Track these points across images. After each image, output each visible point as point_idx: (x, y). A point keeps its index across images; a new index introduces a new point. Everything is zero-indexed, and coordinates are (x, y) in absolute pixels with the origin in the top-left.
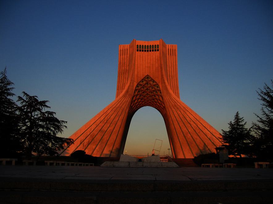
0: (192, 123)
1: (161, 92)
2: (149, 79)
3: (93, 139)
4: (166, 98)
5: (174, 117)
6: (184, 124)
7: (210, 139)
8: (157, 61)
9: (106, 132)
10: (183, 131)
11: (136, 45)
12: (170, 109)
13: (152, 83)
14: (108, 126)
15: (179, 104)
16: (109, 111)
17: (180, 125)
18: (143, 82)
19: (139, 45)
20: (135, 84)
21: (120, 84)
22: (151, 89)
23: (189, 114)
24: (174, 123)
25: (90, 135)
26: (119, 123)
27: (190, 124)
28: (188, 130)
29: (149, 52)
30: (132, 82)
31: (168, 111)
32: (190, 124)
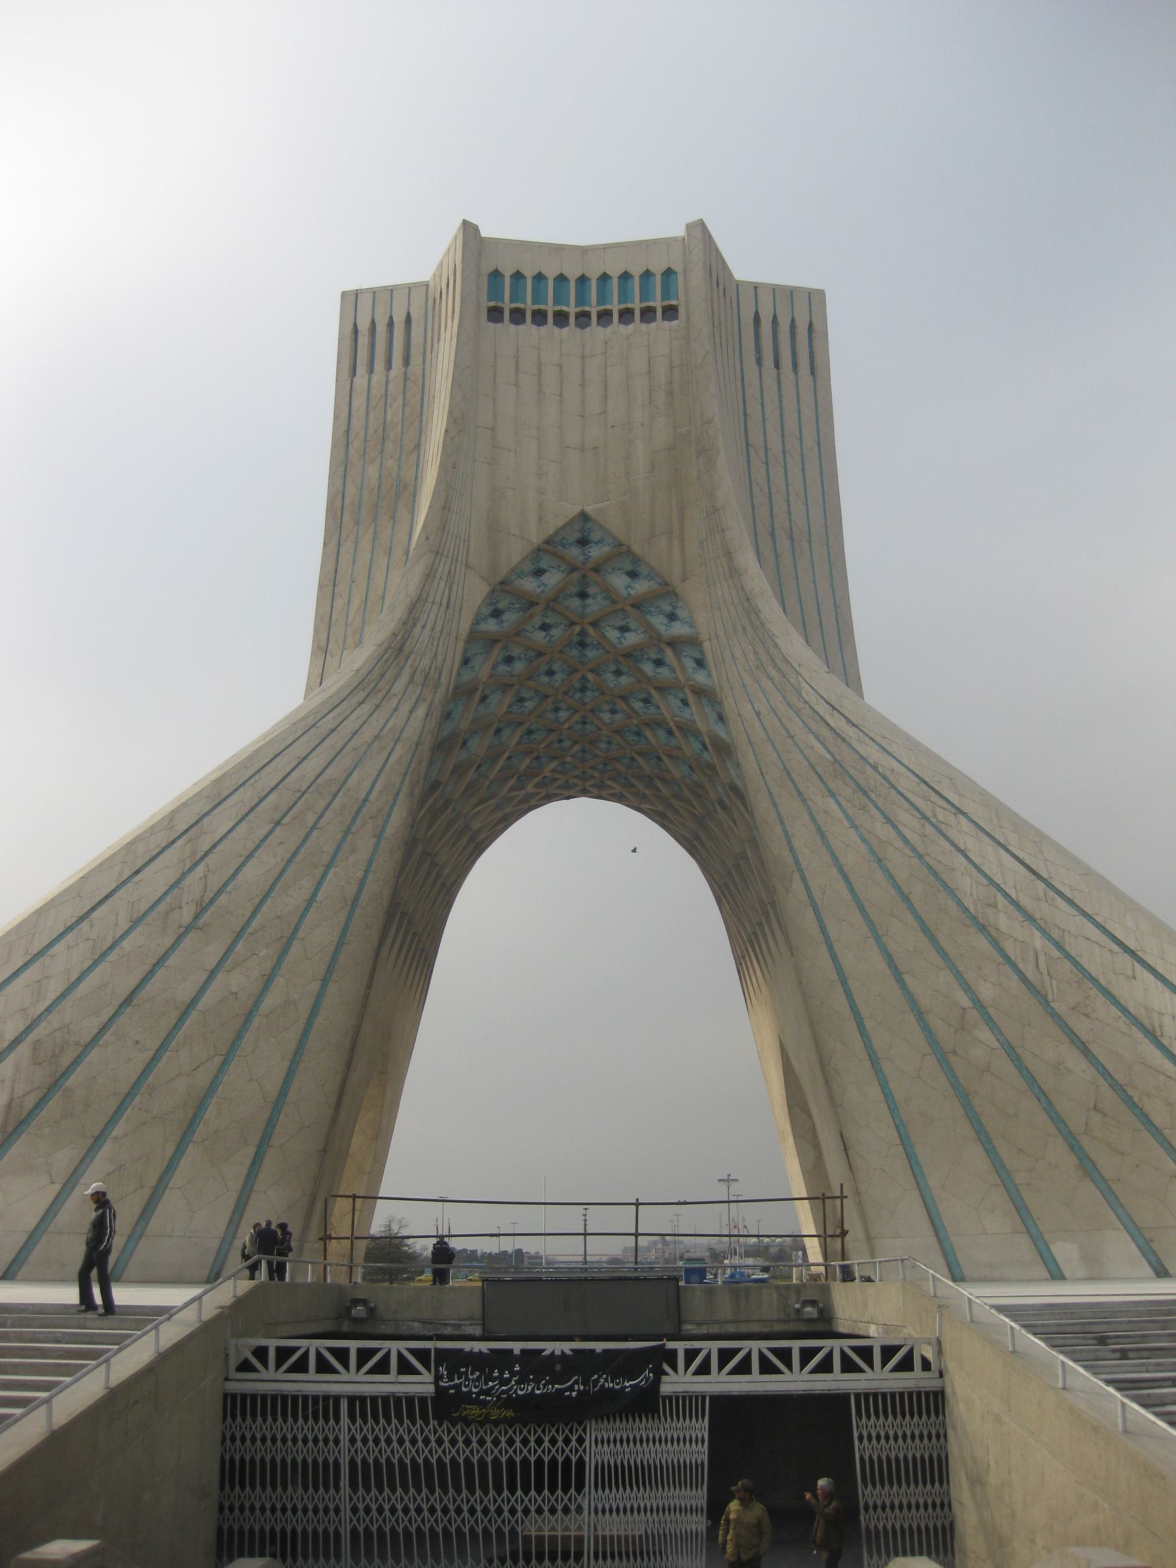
0: (1005, 921)
1: (700, 663)
2: (595, 552)
5: (834, 872)
9: (194, 1015)
11: (488, 268)
13: (619, 581)
15: (874, 755)
16: (222, 821)
18: (539, 573)
19: (508, 272)
20: (475, 592)
21: (339, 603)
22: (613, 635)
24: (833, 934)
25: (24, 1049)
26: (319, 935)
27: (983, 928)
28: (968, 989)
29: (597, 332)
32: (983, 928)
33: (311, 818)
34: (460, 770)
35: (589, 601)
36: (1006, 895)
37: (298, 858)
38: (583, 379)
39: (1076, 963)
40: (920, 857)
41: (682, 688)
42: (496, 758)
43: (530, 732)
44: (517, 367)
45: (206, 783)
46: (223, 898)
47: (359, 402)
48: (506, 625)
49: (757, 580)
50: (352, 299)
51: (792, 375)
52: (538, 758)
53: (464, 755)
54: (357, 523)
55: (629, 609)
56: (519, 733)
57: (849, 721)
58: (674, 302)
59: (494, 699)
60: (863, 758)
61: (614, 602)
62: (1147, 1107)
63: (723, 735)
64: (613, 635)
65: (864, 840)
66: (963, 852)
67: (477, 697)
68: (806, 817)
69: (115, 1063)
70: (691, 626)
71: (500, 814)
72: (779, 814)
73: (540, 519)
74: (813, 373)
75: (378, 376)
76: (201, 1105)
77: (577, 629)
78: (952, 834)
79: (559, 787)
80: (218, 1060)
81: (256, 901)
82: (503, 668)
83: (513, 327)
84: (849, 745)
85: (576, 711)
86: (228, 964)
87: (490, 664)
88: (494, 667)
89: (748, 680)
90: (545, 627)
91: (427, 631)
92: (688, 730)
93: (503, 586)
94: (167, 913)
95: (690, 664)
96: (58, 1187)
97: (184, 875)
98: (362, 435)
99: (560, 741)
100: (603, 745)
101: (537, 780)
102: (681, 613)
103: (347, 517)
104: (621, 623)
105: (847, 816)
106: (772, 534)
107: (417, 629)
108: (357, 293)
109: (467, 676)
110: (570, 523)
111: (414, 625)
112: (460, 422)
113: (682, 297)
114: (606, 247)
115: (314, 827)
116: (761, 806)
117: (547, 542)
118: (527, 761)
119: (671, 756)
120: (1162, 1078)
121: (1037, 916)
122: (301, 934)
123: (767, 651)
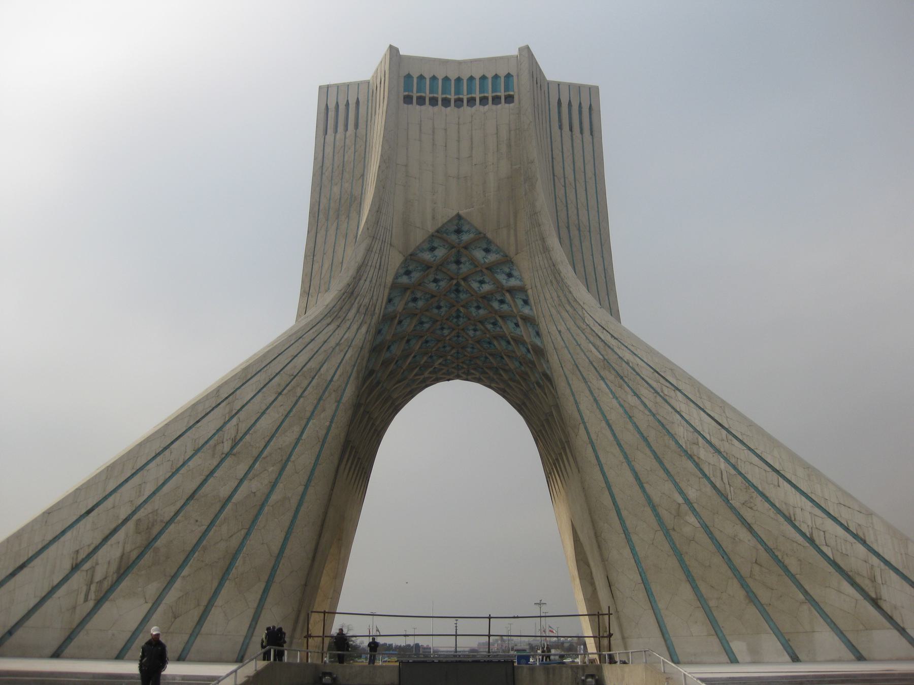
0: (704, 453)
1: (526, 302)
2: (465, 237)
3: (149, 545)
4: (557, 334)
5: (604, 424)
6: (661, 462)
7: (811, 541)
8: (504, 149)
9: (230, 506)
10: (656, 499)
12: (578, 385)
13: (479, 254)
14: (241, 475)
15: (627, 356)
16: (247, 392)
17: (638, 468)
18: (432, 249)
19: (415, 76)
20: (395, 260)
21: (316, 266)
22: (475, 285)
23: (682, 406)
24: (603, 461)
25: (131, 524)
26: (303, 459)
27: (690, 457)
28: (681, 492)
29: (466, 110)
30: (376, 247)
31: (568, 391)
32: (690, 457)
33: (299, 391)
34: (386, 363)
35: (462, 266)
36: (704, 438)
37: (291, 414)
38: (459, 137)
39: (745, 478)
40: (654, 415)
41: (515, 317)
42: (408, 356)
43: (427, 342)
44: (420, 130)
45: (239, 370)
46: (247, 437)
47: (329, 150)
48: (413, 280)
49: (559, 254)
50: (325, 90)
51: (579, 135)
52: (431, 357)
53: (388, 355)
54: (327, 220)
55: (484, 270)
56: (420, 343)
57: (612, 336)
58: (512, 93)
59: (406, 323)
60: (620, 358)
61: (476, 266)
62: (787, 561)
63: (539, 344)
64: (475, 285)
65: (621, 405)
66: (678, 413)
67: (396, 321)
68: (587, 392)
69: (183, 533)
70: (521, 280)
71: (409, 389)
72: (571, 389)
73: (433, 218)
74: (592, 134)
75: (340, 135)
76: (234, 558)
77: (455, 282)
78: (673, 402)
79: (444, 374)
80: (243, 532)
81: (267, 439)
82: (411, 305)
83: (418, 107)
84: (613, 350)
85: (453, 329)
86: (250, 476)
87: (403, 302)
88: (406, 304)
89: (553, 311)
90: (436, 281)
91: (368, 283)
92: (519, 341)
93: (411, 258)
94: (215, 446)
95: (520, 302)
96: (150, 605)
97: (225, 423)
98: (330, 169)
99: (444, 347)
100: (469, 350)
101: (431, 369)
102: (515, 273)
103: (321, 216)
104: (479, 278)
105: (611, 391)
106: (568, 228)
107: (362, 282)
108: (328, 87)
109: (391, 309)
110: (450, 221)
111: (360, 279)
112: (387, 162)
113: (516, 90)
114: (472, 61)
115: (300, 397)
116: (561, 385)
117: (437, 231)
118: (425, 358)
119: (509, 356)
120: (795, 544)
121: (722, 450)
122: (293, 458)
123: (565, 296)
